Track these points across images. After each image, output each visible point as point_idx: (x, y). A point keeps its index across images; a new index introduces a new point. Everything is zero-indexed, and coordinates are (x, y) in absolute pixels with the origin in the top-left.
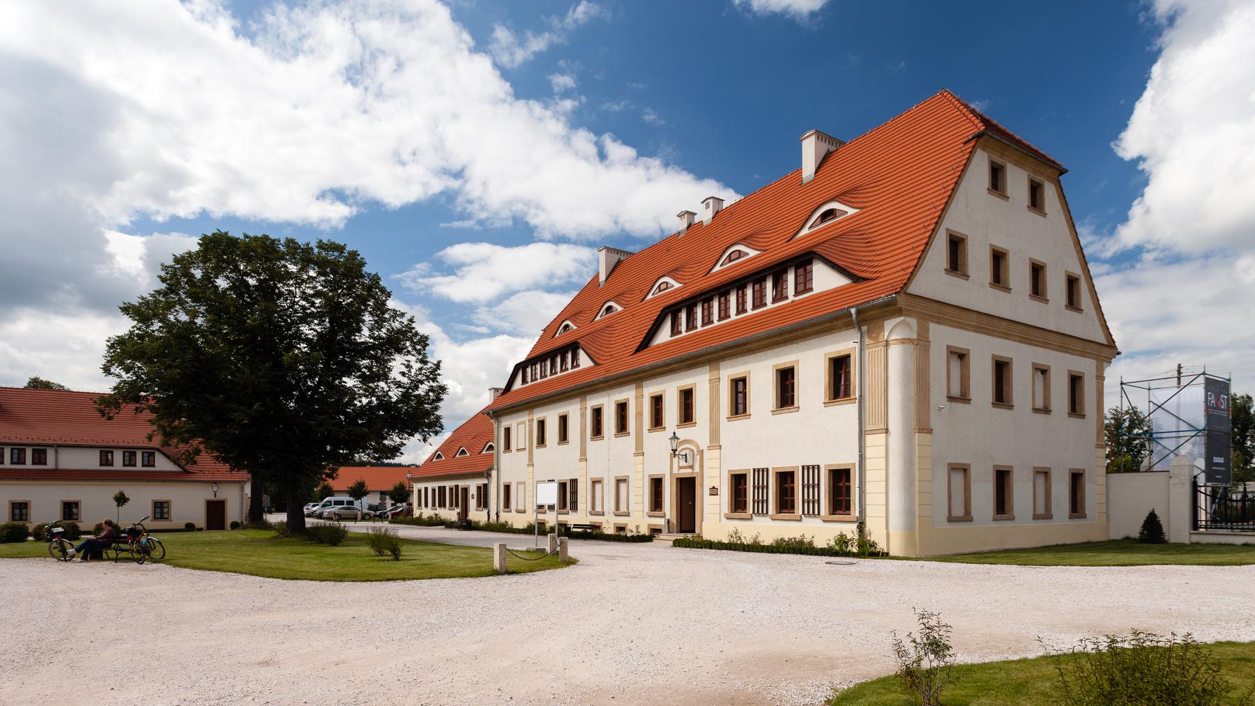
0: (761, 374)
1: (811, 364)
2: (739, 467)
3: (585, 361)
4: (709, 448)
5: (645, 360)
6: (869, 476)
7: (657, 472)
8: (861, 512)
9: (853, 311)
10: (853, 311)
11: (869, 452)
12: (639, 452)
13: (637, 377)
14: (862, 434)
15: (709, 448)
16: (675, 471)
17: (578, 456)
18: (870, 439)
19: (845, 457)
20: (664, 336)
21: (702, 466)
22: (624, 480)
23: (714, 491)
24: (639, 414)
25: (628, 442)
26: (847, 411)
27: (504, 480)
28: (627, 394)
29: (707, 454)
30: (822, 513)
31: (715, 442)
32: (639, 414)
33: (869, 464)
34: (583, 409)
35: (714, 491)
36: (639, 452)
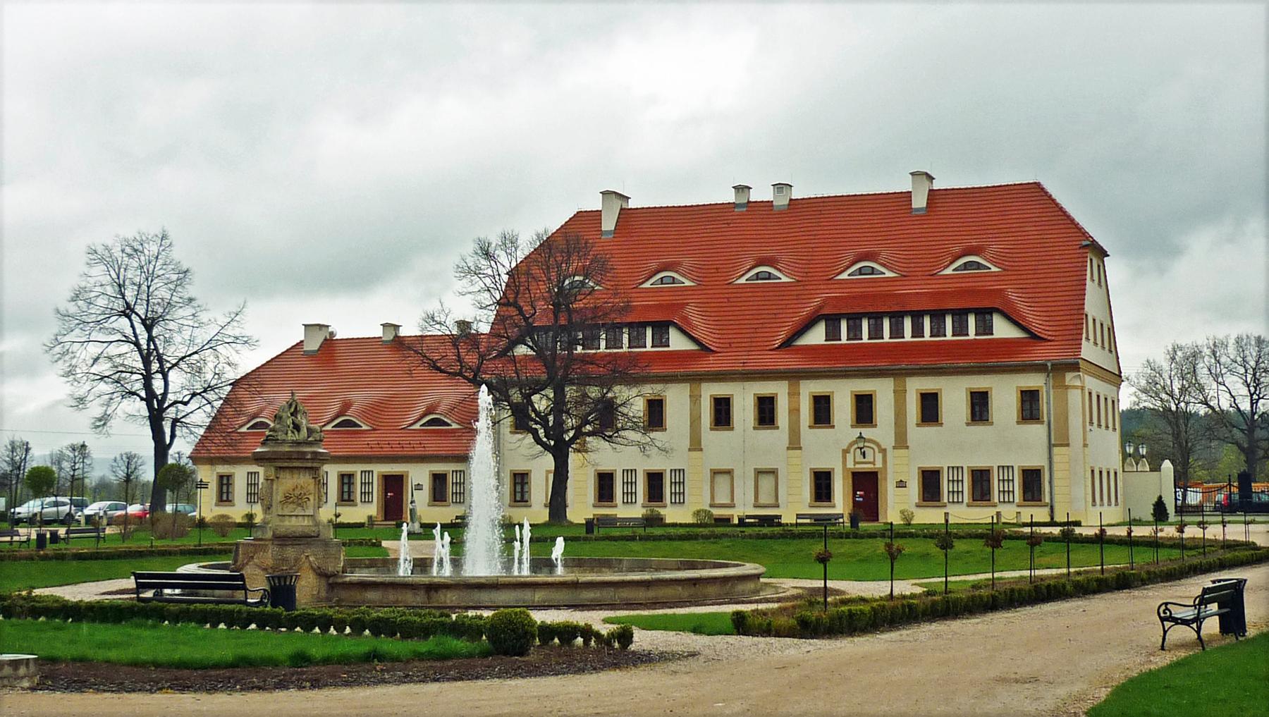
0: (954, 395)
1: (1005, 392)
2: (931, 464)
4: (894, 448)
6: (1056, 475)
7: (822, 465)
8: (1051, 499)
11: (1056, 459)
12: (795, 443)
13: (794, 376)
14: (1050, 446)
15: (894, 448)
16: (850, 465)
17: (687, 443)
18: (1056, 450)
19: (1036, 460)
20: (817, 336)
21: (885, 461)
23: (901, 484)
24: (794, 411)
25: (777, 437)
26: (1037, 432)
28: (779, 389)
29: (890, 453)
30: (1017, 500)
31: (901, 441)
32: (794, 411)
33: (1055, 467)
34: (695, 399)
35: (901, 484)
36: (795, 443)
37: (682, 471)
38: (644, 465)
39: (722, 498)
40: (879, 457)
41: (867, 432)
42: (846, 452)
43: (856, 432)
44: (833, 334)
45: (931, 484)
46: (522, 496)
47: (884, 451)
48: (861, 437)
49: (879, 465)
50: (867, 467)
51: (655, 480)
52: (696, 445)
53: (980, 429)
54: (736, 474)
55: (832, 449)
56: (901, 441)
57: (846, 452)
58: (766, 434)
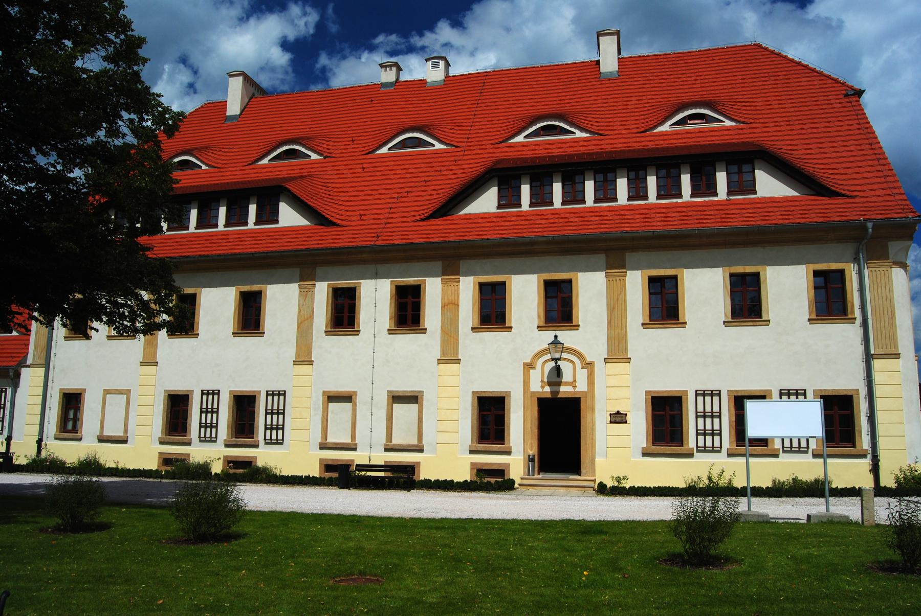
2: (667, 385)
3: (289, 217)
4: (606, 361)
5: (440, 231)
7: (491, 387)
9: (870, 225)
10: (870, 225)
11: (878, 378)
12: (450, 357)
14: (869, 358)
15: (606, 361)
17: (291, 353)
18: (877, 364)
19: (848, 380)
20: (487, 202)
22: (413, 398)
24: (450, 306)
25: (422, 347)
27: (62, 382)
29: (599, 367)
31: (618, 352)
32: (450, 306)
33: (878, 391)
35: (618, 418)
36: (450, 357)
37: (282, 394)
38: (230, 385)
39: (337, 435)
40: (582, 375)
41: (566, 337)
42: (529, 366)
43: (549, 336)
44: (509, 198)
45: (667, 420)
46: (74, 426)
47: (589, 366)
48: (555, 342)
49: (582, 386)
50: (565, 390)
51: (244, 405)
52: (304, 358)
53: (747, 333)
54: (359, 399)
55: (510, 361)
56: (618, 352)
57: (529, 366)
58: (407, 341)
